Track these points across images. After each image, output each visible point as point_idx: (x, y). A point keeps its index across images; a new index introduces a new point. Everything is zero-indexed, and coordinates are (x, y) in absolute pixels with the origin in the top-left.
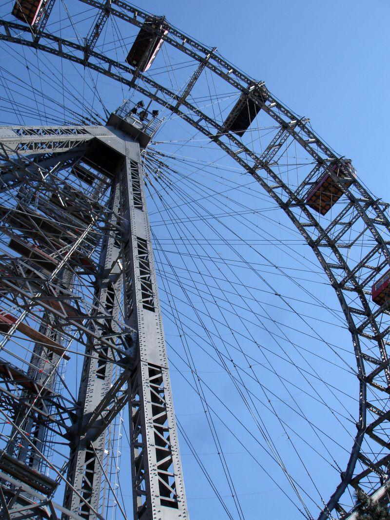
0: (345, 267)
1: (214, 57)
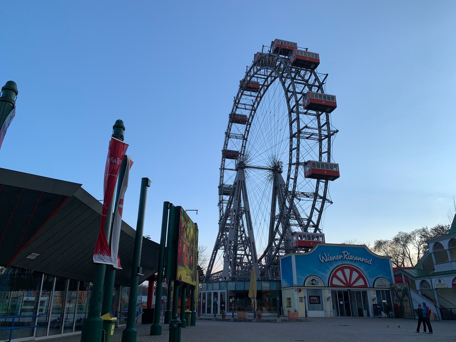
0: (256, 99)
1: (222, 167)
